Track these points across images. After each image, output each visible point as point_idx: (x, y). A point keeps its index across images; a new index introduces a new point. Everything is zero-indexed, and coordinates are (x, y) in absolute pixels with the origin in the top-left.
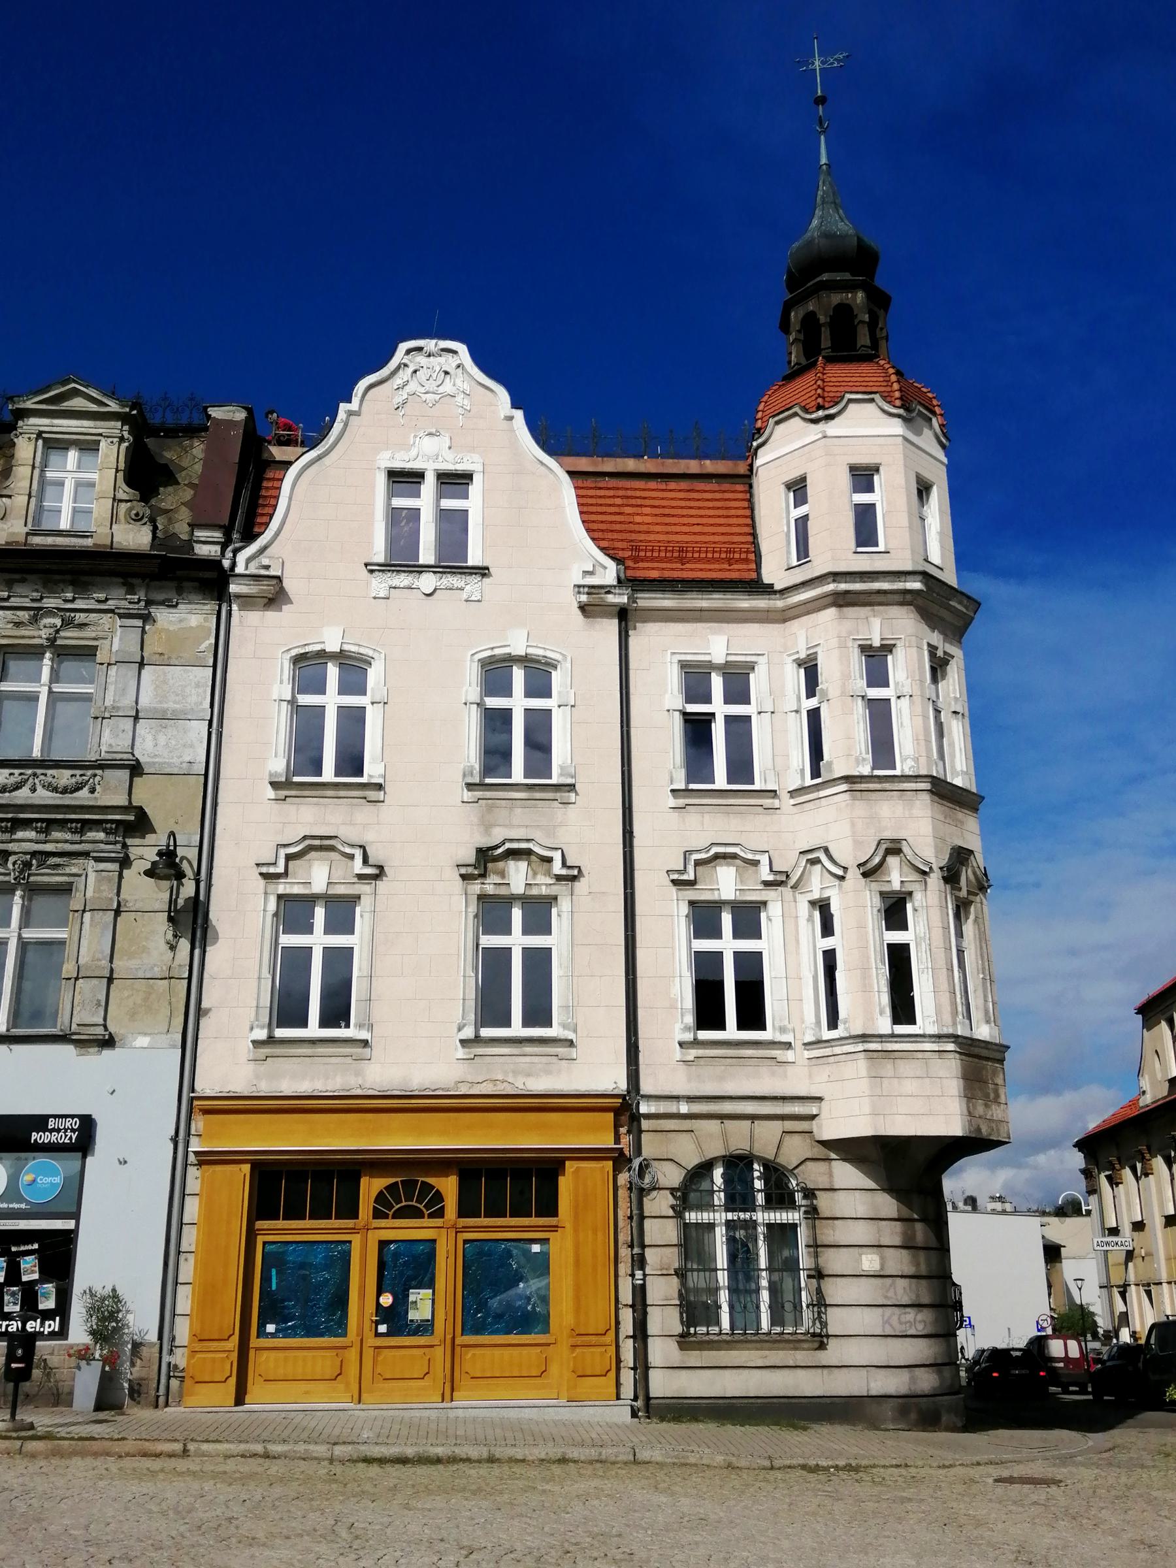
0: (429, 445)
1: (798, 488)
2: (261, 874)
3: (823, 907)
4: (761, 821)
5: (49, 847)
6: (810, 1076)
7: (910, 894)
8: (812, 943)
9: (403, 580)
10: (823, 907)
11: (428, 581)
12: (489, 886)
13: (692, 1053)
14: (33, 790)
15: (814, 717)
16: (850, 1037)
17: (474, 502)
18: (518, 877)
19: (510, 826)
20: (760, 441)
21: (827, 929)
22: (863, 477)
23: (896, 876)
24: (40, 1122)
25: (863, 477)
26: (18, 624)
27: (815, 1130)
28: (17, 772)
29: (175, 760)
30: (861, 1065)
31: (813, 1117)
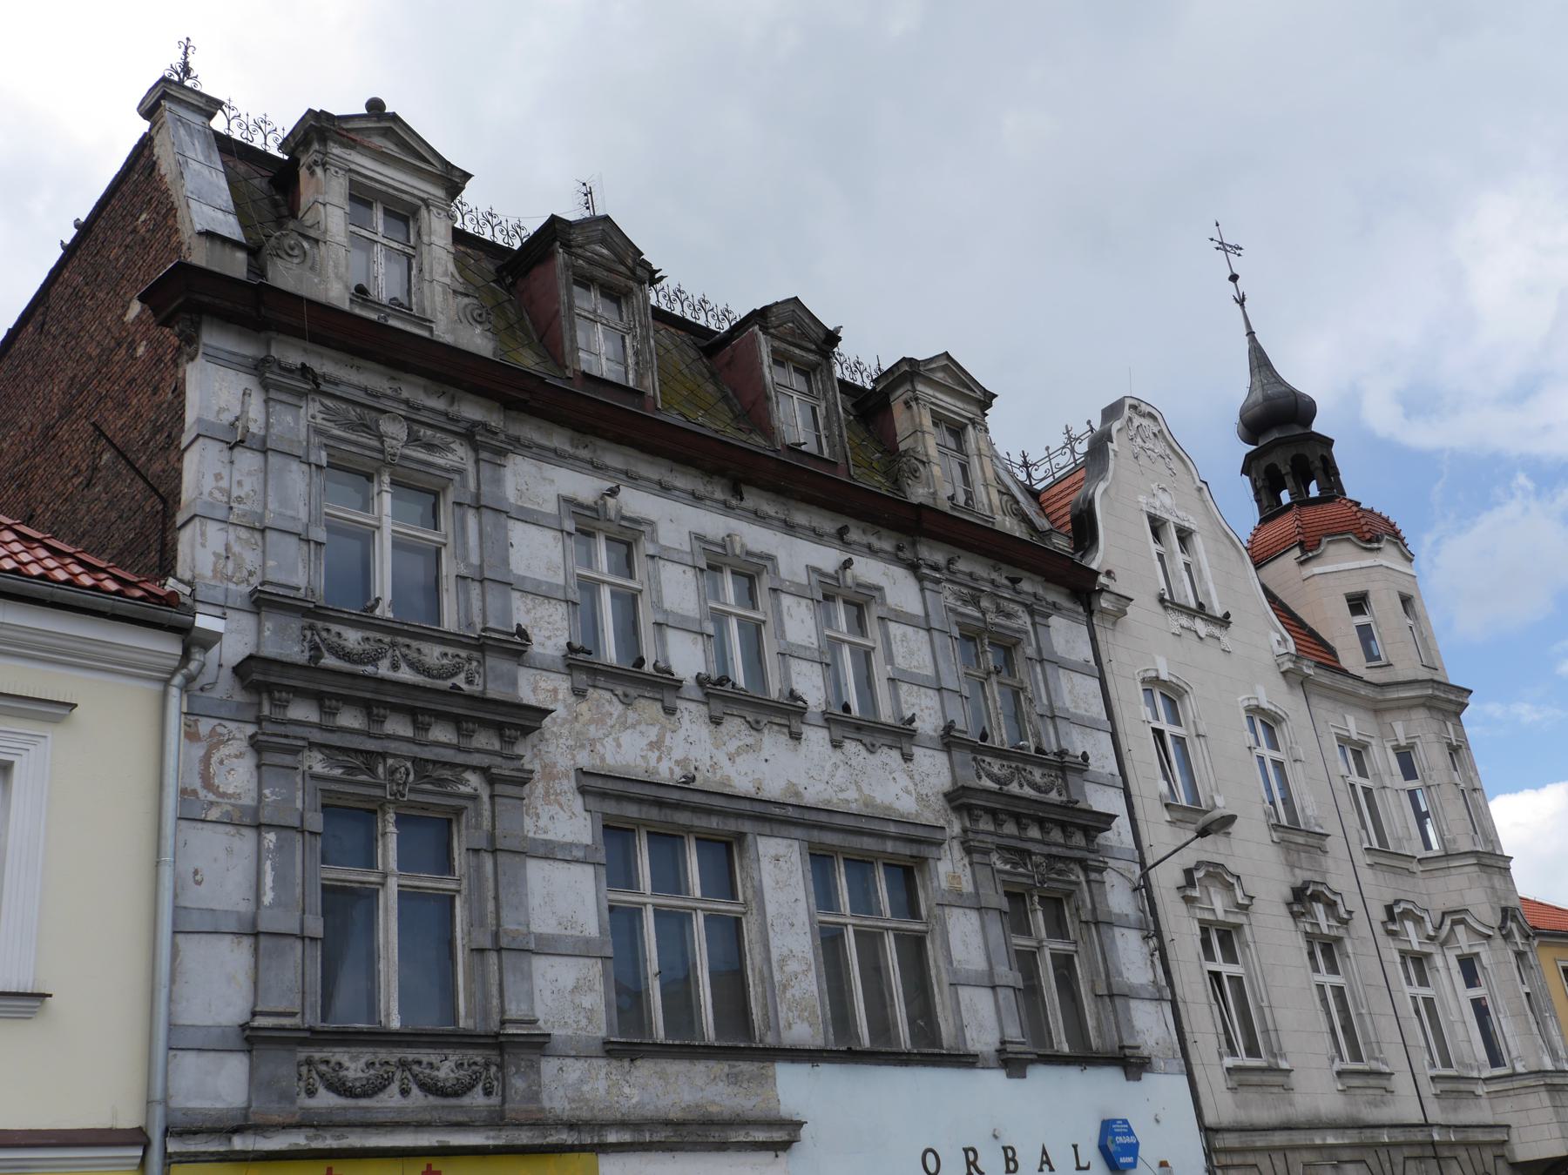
2: (1183, 897)
5: (1054, 850)
6: (1492, 1108)
7: (1477, 954)
13: (1442, 1086)
14: (1021, 786)
16: (1531, 1073)
19: (1301, 868)
20: (1315, 553)
21: (1471, 979)
26: (965, 602)
27: (1507, 1154)
28: (1005, 763)
29: (1101, 770)
30: (1544, 1096)
31: (1504, 1142)
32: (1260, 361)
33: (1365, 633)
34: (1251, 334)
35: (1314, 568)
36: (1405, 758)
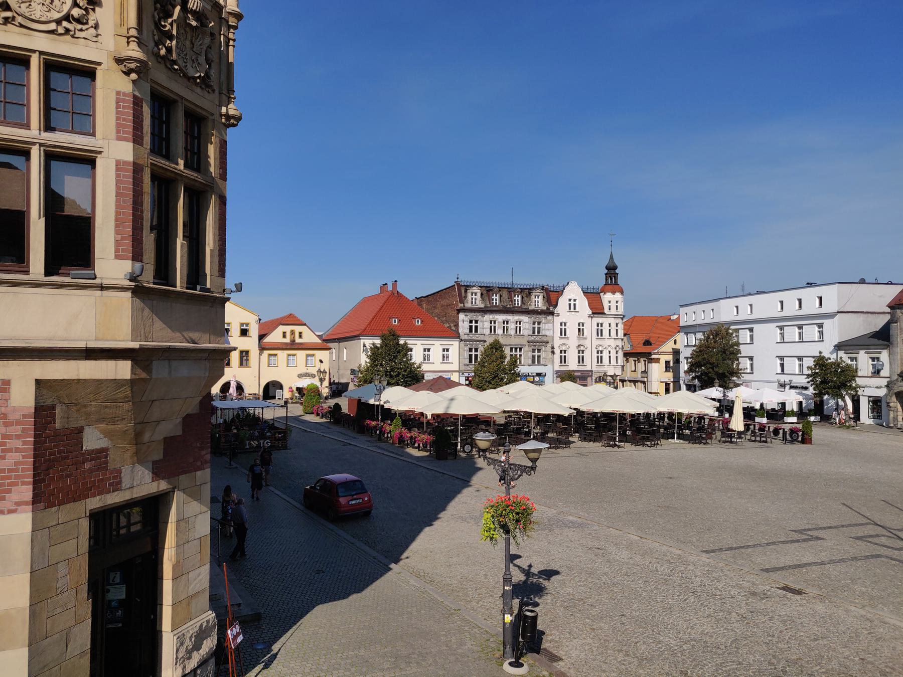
0: (573, 295)
1: (610, 302)
3: (610, 352)
4: (603, 341)
8: (608, 355)
9: (571, 313)
10: (610, 352)
11: (573, 313)
12: (579, 349)
15: (610, 330)
17: (577, 302)
18: (582, 348)
21: (610, 353)
22: (617, 302)
23: (618, 349)
24: (542, 373)
25: (617, 302)
30: (613, 368)
32: (612, 257)
33: (610, 306)
34: (612, 253)
35: (605, 296)
36: (610, 324)
